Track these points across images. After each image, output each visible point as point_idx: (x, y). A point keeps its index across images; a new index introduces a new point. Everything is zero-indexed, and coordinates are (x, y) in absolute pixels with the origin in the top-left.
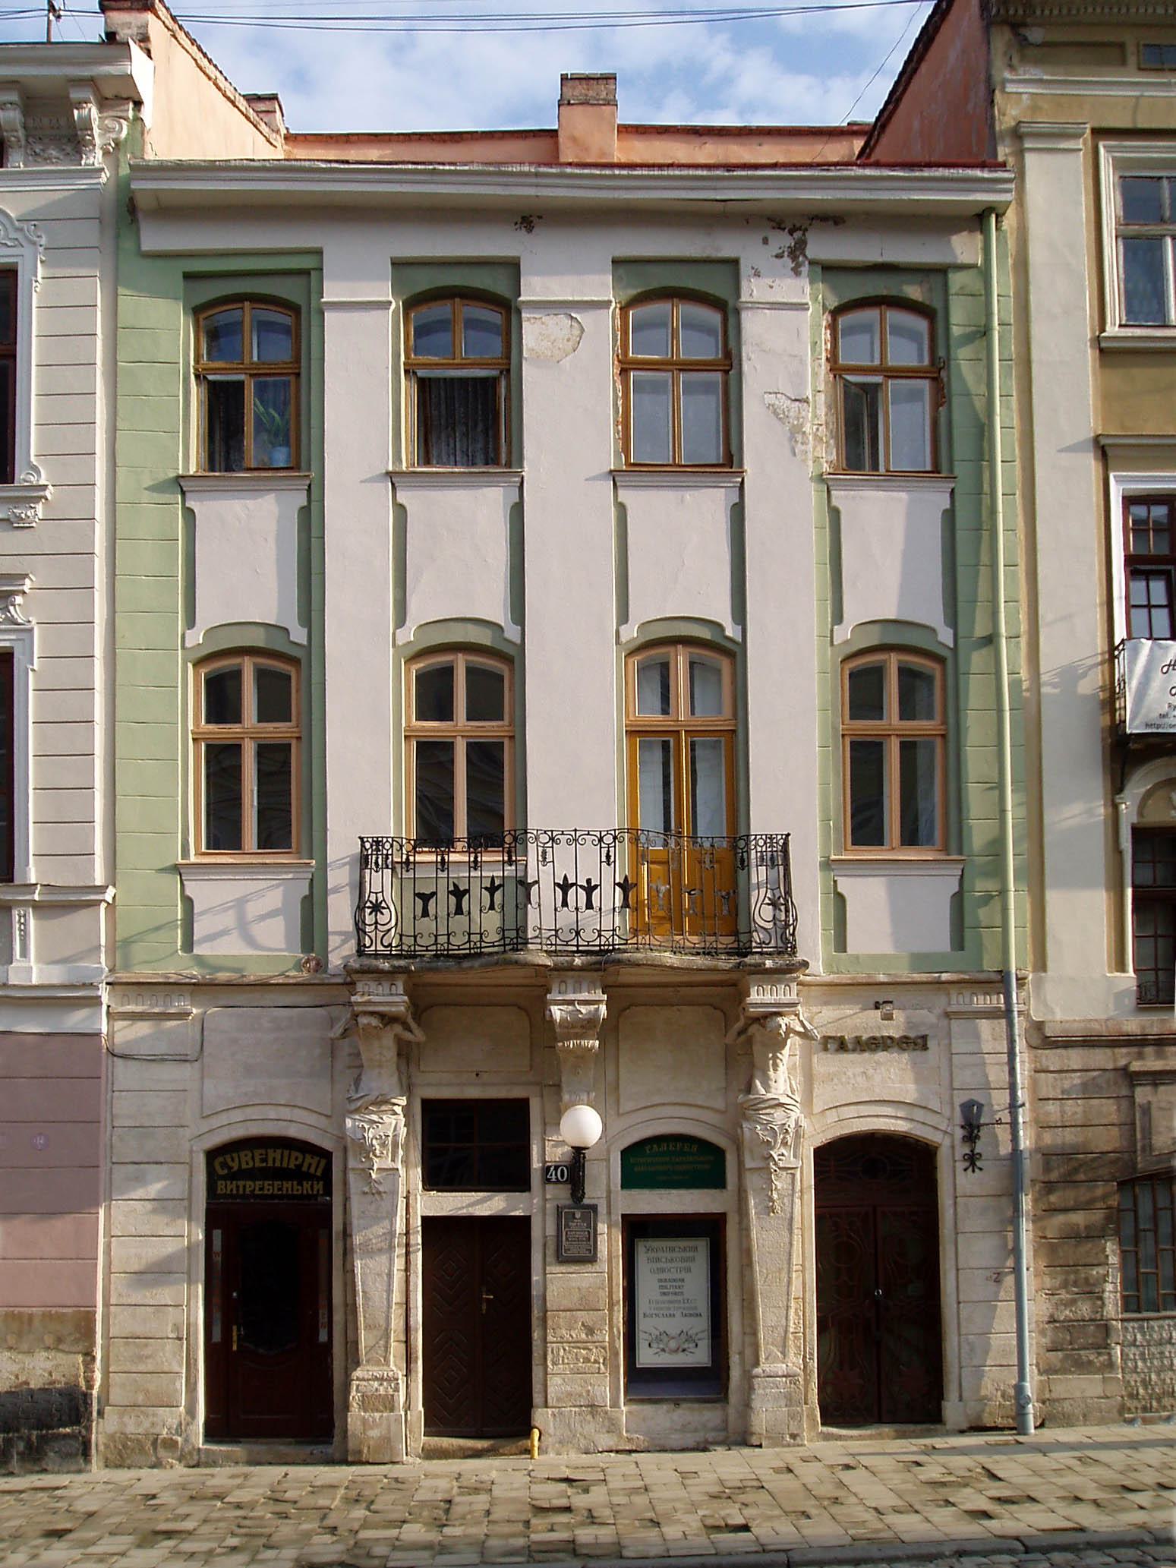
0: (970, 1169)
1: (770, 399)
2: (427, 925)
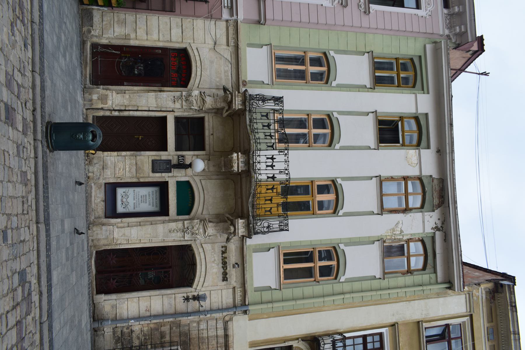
0: (184, 298)
1: (401, 222)
2: (259, 116)
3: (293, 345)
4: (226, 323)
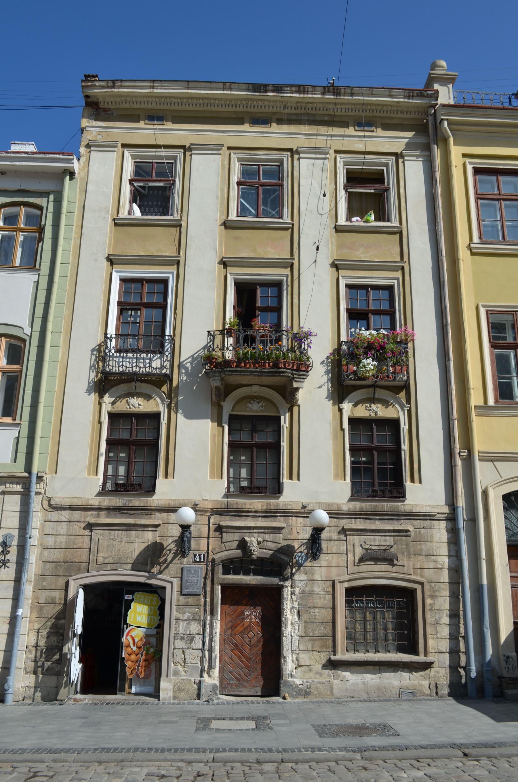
3: (108, 411)
4: (54, 508)
